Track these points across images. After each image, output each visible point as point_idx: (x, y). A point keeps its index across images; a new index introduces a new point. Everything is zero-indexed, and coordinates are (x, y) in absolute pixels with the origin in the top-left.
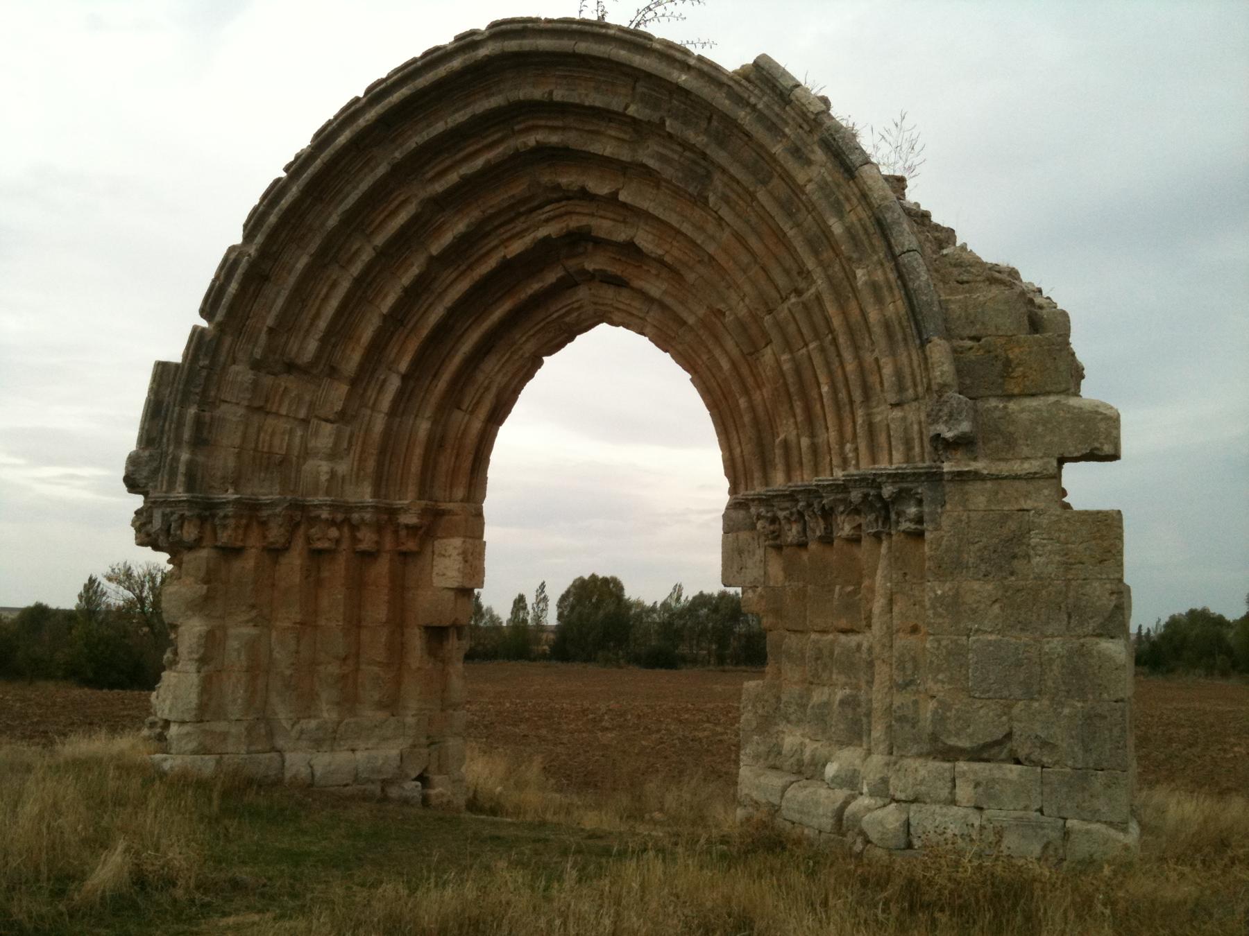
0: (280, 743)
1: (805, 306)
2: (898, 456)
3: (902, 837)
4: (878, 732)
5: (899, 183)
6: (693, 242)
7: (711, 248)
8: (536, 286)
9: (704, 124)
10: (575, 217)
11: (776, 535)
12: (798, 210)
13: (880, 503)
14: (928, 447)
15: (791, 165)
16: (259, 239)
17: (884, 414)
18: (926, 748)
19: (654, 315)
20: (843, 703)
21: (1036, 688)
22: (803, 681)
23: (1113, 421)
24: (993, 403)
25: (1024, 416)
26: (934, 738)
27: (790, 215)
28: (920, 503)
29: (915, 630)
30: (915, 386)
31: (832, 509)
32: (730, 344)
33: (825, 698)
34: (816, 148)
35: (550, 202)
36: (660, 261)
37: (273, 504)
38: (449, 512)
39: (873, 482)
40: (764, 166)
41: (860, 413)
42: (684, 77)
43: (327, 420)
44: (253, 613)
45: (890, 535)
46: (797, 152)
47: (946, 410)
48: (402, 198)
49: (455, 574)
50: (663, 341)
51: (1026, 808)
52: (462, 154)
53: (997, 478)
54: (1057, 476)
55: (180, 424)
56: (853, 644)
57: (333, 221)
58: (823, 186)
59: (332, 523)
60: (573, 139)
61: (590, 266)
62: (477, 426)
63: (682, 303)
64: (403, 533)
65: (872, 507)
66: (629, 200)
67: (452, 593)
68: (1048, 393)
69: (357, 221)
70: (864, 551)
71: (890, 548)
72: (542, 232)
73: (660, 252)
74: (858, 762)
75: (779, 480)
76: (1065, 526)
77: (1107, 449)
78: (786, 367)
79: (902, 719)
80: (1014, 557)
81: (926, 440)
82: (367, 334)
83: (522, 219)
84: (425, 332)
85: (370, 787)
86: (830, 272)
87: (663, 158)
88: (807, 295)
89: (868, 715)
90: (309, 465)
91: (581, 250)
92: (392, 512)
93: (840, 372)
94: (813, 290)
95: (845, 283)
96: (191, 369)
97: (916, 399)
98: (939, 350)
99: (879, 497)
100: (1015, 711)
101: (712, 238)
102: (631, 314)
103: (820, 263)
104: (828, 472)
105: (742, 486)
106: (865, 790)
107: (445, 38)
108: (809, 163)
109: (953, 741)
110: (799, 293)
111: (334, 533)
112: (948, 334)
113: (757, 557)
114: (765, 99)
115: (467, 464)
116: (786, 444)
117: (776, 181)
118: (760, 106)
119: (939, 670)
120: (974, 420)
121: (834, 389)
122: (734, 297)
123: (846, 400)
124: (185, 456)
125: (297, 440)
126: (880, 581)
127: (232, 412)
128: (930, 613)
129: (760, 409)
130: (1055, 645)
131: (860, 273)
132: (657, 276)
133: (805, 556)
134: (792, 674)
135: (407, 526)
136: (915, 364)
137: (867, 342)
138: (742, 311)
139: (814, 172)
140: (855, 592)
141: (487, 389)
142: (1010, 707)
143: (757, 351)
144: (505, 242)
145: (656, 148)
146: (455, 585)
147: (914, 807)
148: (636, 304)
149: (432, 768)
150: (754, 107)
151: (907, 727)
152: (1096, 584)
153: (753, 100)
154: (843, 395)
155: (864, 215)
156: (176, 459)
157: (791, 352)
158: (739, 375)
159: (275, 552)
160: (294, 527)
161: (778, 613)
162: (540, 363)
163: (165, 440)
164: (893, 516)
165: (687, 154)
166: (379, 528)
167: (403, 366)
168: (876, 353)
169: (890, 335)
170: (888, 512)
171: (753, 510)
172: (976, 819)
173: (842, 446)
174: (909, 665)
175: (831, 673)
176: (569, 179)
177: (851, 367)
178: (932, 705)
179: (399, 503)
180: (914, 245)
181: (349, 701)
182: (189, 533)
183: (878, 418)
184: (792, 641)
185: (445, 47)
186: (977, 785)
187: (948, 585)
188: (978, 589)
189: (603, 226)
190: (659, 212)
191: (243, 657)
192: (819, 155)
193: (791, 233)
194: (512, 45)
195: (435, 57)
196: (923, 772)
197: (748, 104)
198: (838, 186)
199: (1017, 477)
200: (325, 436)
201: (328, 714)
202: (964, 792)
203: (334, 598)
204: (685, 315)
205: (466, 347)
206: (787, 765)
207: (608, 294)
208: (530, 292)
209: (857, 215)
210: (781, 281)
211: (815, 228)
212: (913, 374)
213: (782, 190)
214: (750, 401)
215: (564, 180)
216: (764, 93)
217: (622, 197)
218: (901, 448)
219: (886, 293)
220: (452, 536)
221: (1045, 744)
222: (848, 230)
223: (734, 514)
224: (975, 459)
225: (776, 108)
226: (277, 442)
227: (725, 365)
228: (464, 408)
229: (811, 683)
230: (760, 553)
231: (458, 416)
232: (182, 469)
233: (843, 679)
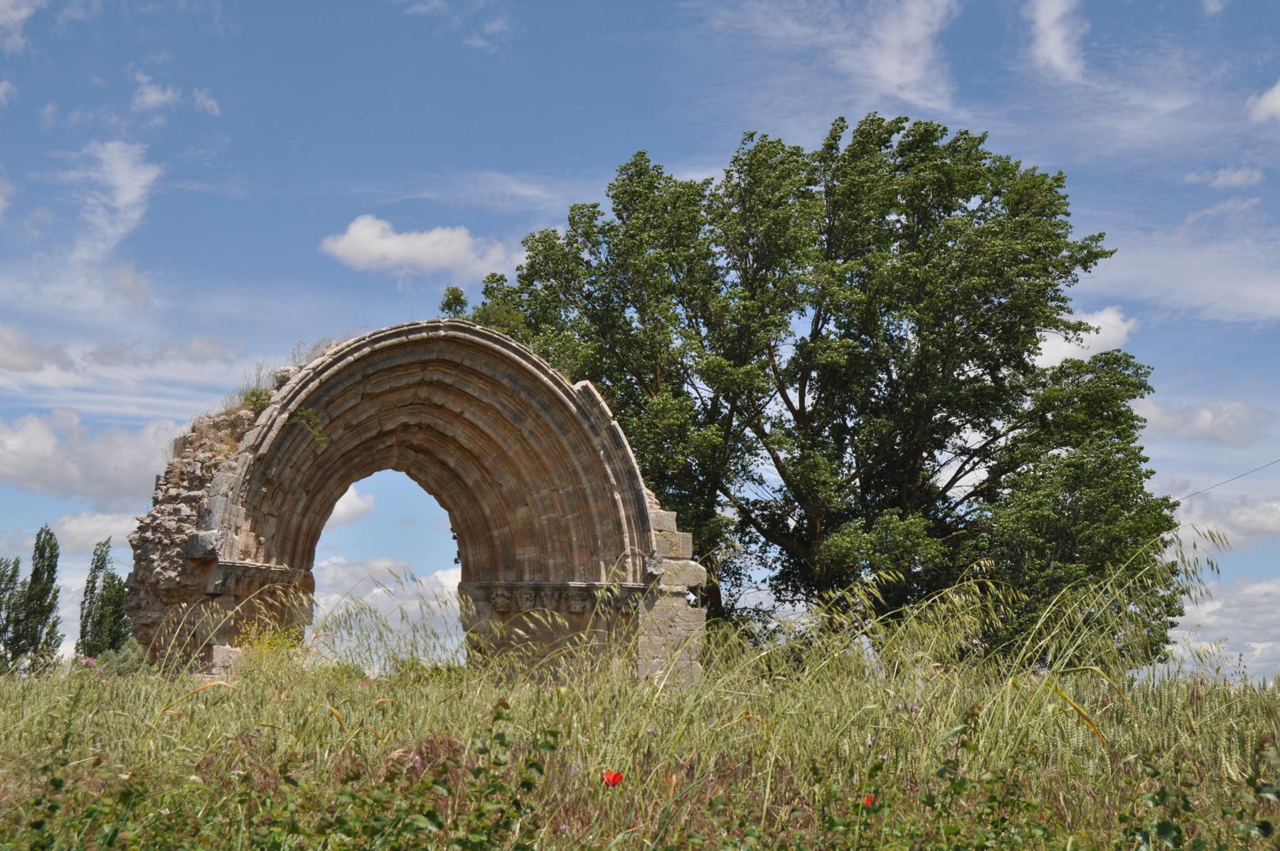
7: (511, 454)
8: (381, 446)
19: (435, 470)
46: (592, 427)
176: (438, 399)
189: (440, 423)
192: (604, 434)
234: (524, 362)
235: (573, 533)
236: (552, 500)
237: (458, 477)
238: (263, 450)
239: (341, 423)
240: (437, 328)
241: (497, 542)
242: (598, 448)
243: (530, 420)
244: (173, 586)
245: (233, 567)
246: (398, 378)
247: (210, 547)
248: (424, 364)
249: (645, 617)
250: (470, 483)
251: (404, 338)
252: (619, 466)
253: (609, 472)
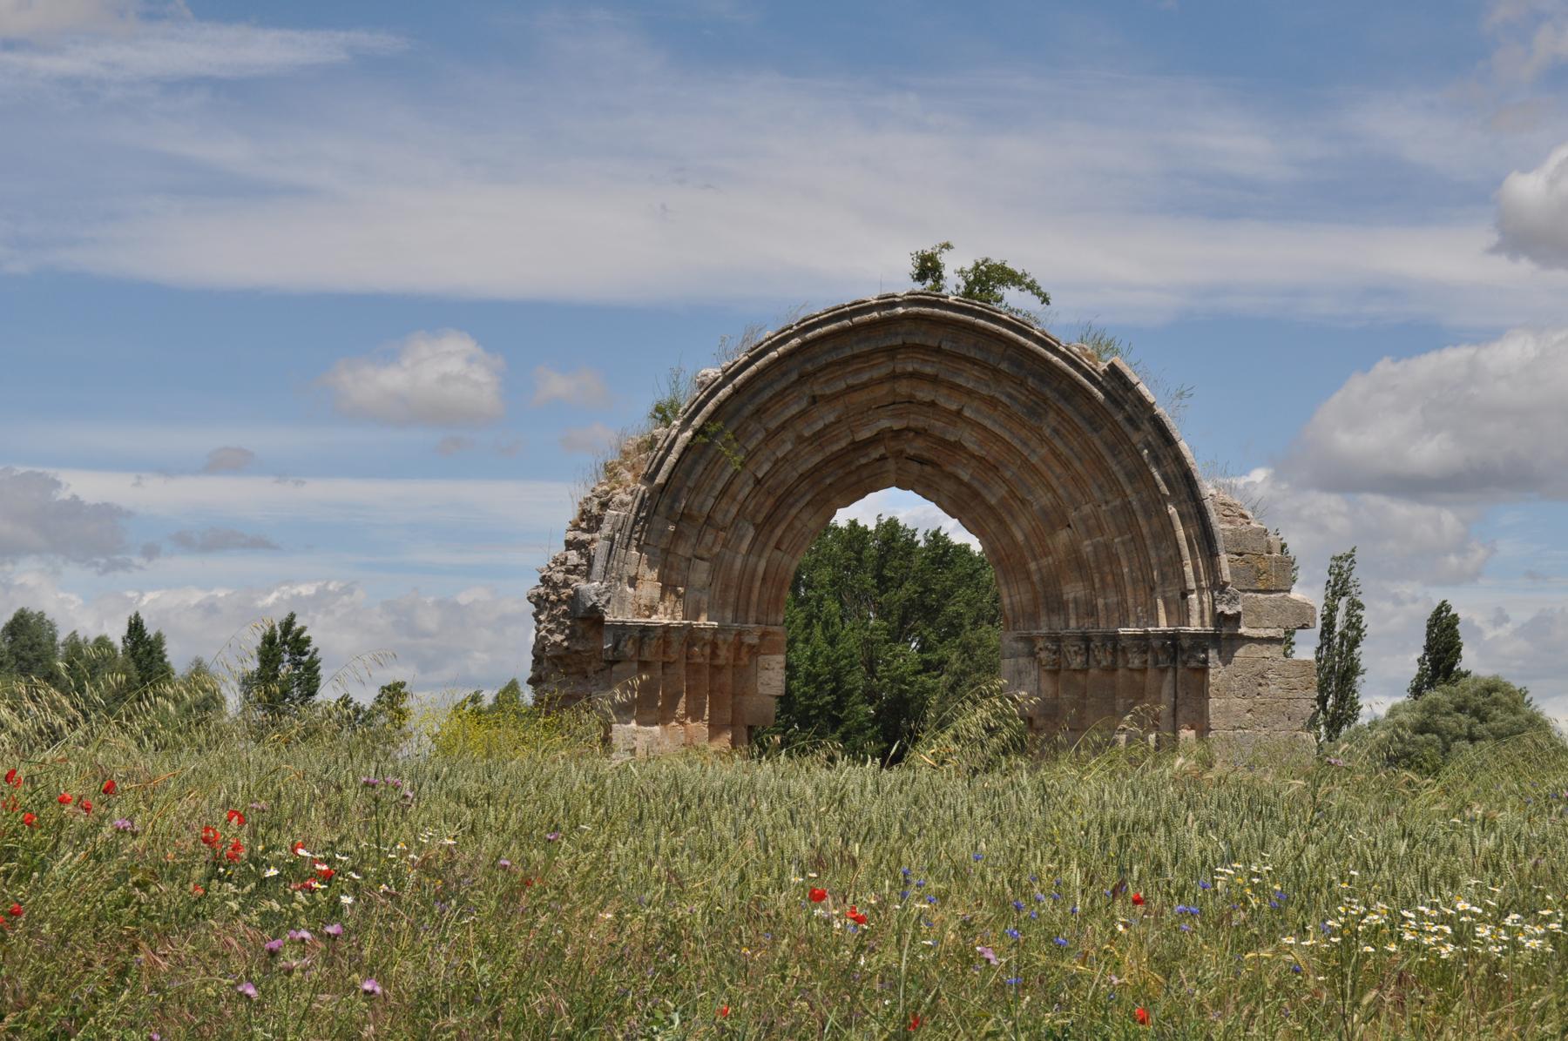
7: (1034, 460)
8: (863, 461)
38: (774, 633)
46: (1130, 420)
63: (985, 486)
72: (885, 424)
87: (1010, 396)
107: (872, 297)
117: (1105, 432)
159: (665, 665)
176: (924, 393)
189: (938, 425)
192: (1147, 426)
217: (967, 413)
228: (784, 547)
230: (1034, 673)
234: (1022, 339)
235: (1124, 563)
236: (1097, 519)
237: (976, 495)
238: (660, 479)
239: (789, 435)
240: (894, 305)
241: (1036, 578)
242: (1140, 446)
243: (1052, 415)
244: (561, 652)
245: (623, 626)
246: (858, 371)
247: (589, 604)
248: (892, 352)
249: (1217, 673)
250: (993, 502)
251: (846, 322)
252: (1171, 468)
253: (1158, 477)
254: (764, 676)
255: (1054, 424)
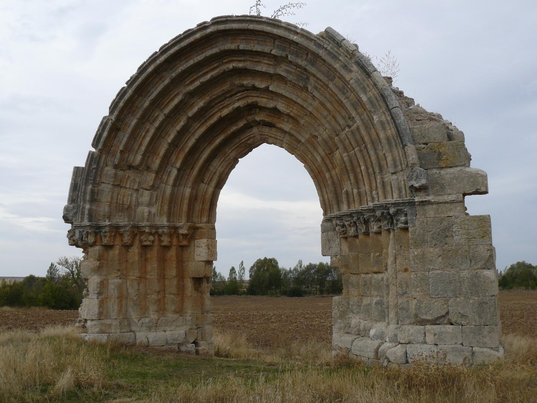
0: (134, 328)
1: (352, 132)
2: (396, 195)
3: (404, 358)
4: (392, 315)
5: (389, 80)
6: (302, 107)
7: (310, 109)
8: (234, 128)
9: (305, 57)
10: (250, 98)
11: (345, 232)
12: (347, 91)
13: (389, 216)
14: (408, 191)
15: (343, 72)
16: (116, 113)
17: (389, 178)
18: (413, 320)
19: (287, 138)
20: (376, 303)
21: (458, 292)
22: (359, 295)
23: (484, 177)
24: (435, 171)
25: (448, 176)
26: (416, 316)
27: (344, 94)
28: (406, 215)
29: (406, 270)
30: (401, 165)
31: (368, 219)
32: (320, 150)
33: (368, 302)
34: (354, 65)
35: (240, 92)
36: (288, 115)
37: (125, 226)
38: (201, 228)
39: (386, 207)
40: (332, 74)
41: (378, 177)
42: (295, 37)
43: (146, 189)
44: (119, 273)
45: (394, 230)
46: (345, 67)
47: (415, 175)
48: (175, 93)
49: (204, 254)
50: (292, 150)
51: (456, 343)
52: (200, 74)
53: (438, 203)
54: (463, 201)
55: (85, 193)
56: (380, 278)
57: (147, 104)
58: (357, 81)
59: (151, 234)
60: (248, 65)
61: (258, 119)
62: (211, 190)
64: (181, 237)
65: (385, 218)
66: (274, 90)
67: (203, 263)
68: (457, 166)
69: (157, 103)
70: (383, 238)
71: (394, 235)
72: (236, 105)
73: (288, 111)
74: (384, 328)
75: (345, 209)
76: (467, 222)
77: (483, 189)
78: (345, 159)
79: (402, 309)
80: (447, 237)
81: (407, 188)
82: (162, 152)
83: (228, 100)
84: (187, 150)
85: (173, 347)
86: (362, 117)
87: (287, 71)
88: (352, 128)
89: (388, 308)
90: (140, 209)
91: (253, 112)
92: (176, 228)
93: (369, 160)
94: (355, 125)
95: (369, 122)
96: (89, 169)
97: (402, 171)
98: (411, 149)
99: (389, 213)
100: (450, 303)
101: (311, 104)
102: (277, 139)
103: (358, 113)
104: (366, 204)
105: (329, 212)
106: (387, 340)
107: (193, 26)
108: (351, 71)
109: (424, 317)
110: (349, 127)
111: (151, 238)
112: (414, 142)
113: (337, 243)
114: (331, 45)
115: (207, 207)
116: (347, 193)
117: (337, 79)
118: (329, 48)
119: (417, 287)
120: (427, 179)
121: (367, 168)
122: (321, 130)
123: (372, 172)
124: (87, 206)
125: (134, 198)
126: (391, 250)
127: (106, 188)
128: (412, 262)
129: (335, 178)
130: (465, 274)
131: (375, 117)
132: (287, 122)
133: (357, 241)
134: (354, 292)
135: (182, 234)
136: (401, 155)
137: (380, 147)
138: (325, 136)
139: (353, 75)
140: (380, 256)
141: (215, 173)
142: (448, 301)
143: (332, 152)
144: (220, 110)
145: (284, 67)
146: (205, 259)
147: (408, 346)
148: (279, 134)
149: (199, 338)
150: (326, 49)
151: (404, 312)
152: (481, 247)
153: (325, 46)
154: (371, 170)
155: (375, 93)
156: (84, 208)
157: (347, 152)
158: (325, 163)
159: (127, 247)
160: (134, 236)
161: (347, 266)
162: (238, 162)
163: (79, 200)
164: (395, 221)
165: (298, 69)
166: (171, 236)
167: (178, 165)
168: (384, 151)
169: (389, 144)
170: (392, 220)
171: (334, 222)
172: (435, 349)
173: (371, 192)
174: (404, 286)
175: (371, 291)
176: (247, 82)
177: (373, 158)
178: (415, 302)
179: (179, 224)
180: (398, 105)
181: (162, 310)
182: (91, 239)
183: (386, 180)
184: (354, 278)
185: (193, 29)
186: (435, 335)
187: (419, 250)
188: (432, 251)
189: (263, 101)
190: (287, 95)
191: (116, 292)
192: (355, 68)
193: (344, 101)
194: (221, 27)
195: (189, 34)
196: (412, 331)
197: (323, 47)
198: (364, 81)
199: (446, 203)
200: (146, 196)
201: (154, 316)
202: (430, 338)
203: (153, 266)
204: (300, 138)
205: (205, 156)
206: (353, 332)
207: (266, 130)
208: (232, 131)
209: (373, 93)
210: (342, 122)
211: (355, 99)
212: (400, 160)
213: (340, 84)
214: (331, 175)
215: (245, 83)
216: (330, 43)
217: (270, 89)
218: (397, 192)
219: (387, 125)
220: (202, 238)
221: (463, 316)
222: (369, 99)
223: (325, 224)
224: (428, 195)
225: (335, 49)
226: (125, 199)
227: (319, 159)
228: (205, 182)
229: (362, 296)
230: (338, 240)
231: (203, 186)
232: (86, 212)
233: (376, 293)
254: (198, 251)
255: (313, 82)
